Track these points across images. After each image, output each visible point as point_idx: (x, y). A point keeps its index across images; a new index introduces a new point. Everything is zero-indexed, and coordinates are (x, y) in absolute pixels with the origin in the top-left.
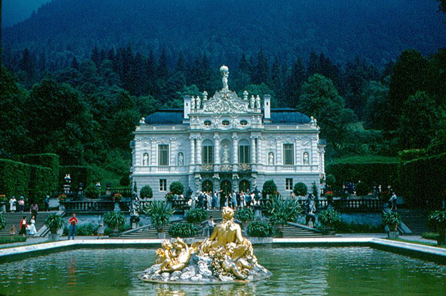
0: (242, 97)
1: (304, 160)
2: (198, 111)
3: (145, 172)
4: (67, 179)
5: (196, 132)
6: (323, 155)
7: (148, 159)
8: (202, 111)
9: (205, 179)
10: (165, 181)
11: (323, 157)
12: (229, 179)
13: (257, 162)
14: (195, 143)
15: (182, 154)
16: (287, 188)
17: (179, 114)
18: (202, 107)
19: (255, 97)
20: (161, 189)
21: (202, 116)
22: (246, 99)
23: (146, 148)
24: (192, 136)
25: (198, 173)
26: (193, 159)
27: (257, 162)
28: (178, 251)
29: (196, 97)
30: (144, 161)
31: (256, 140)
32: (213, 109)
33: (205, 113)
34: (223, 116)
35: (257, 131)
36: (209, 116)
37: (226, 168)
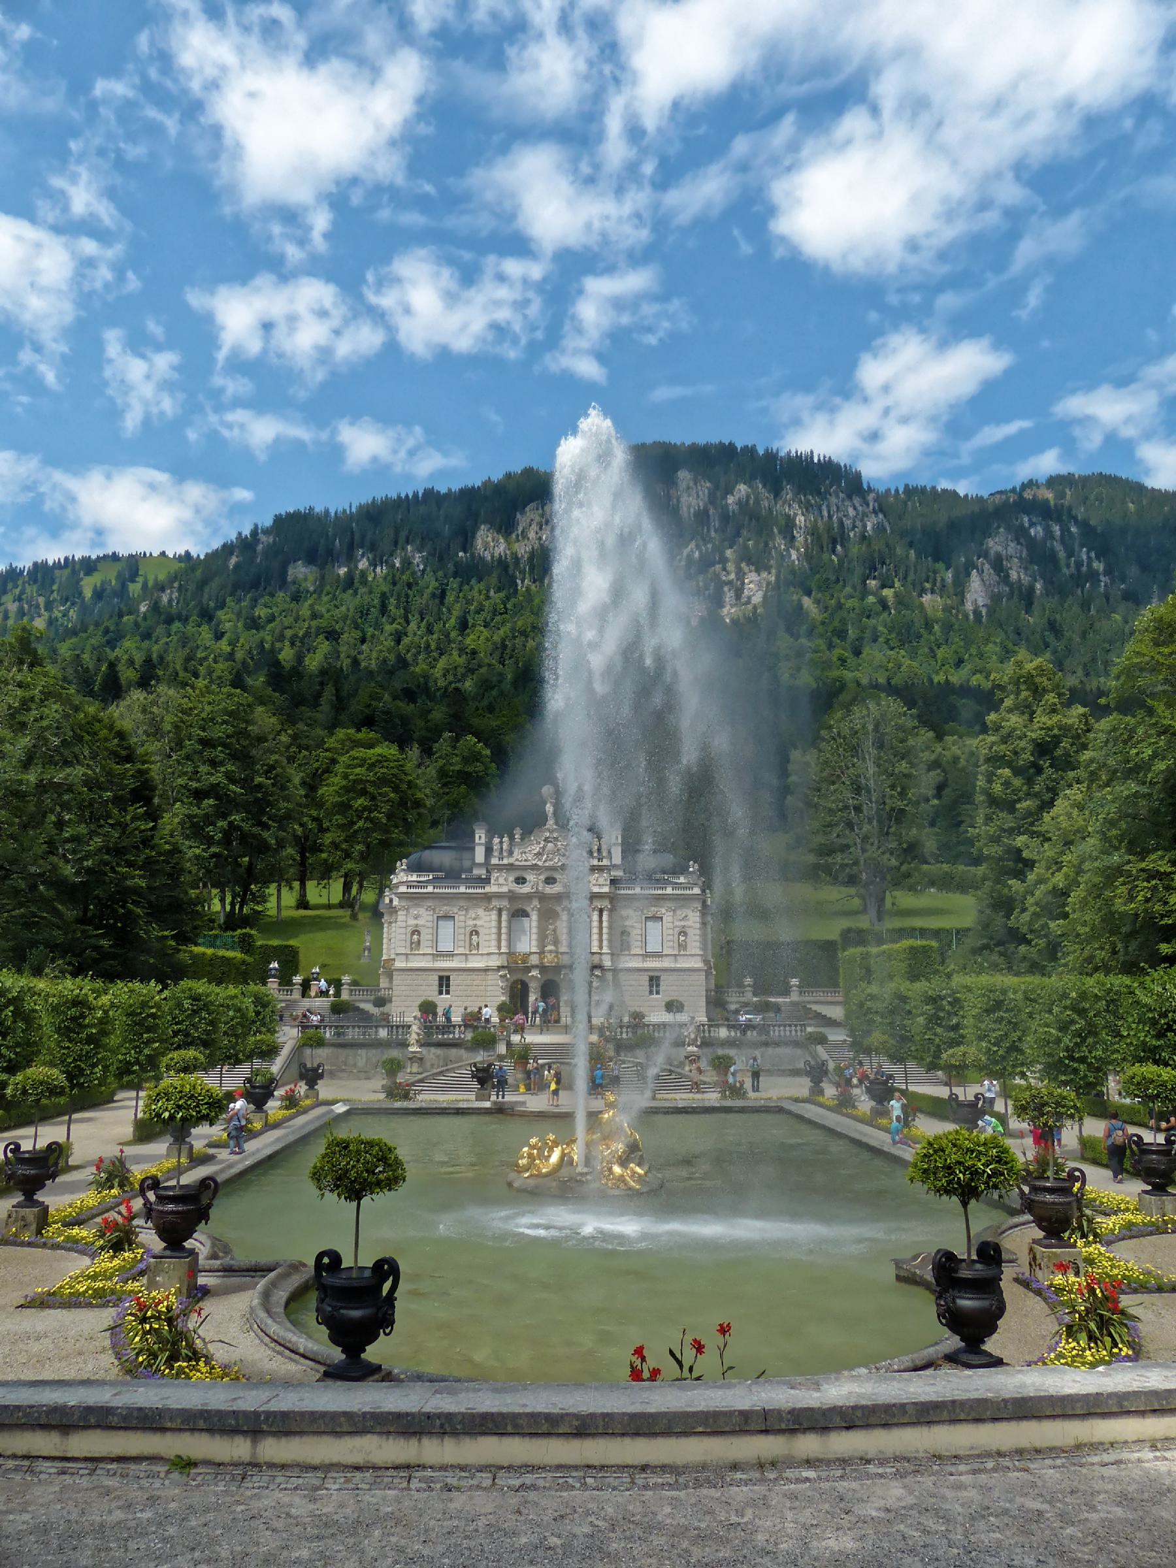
2: (505, 861)
4: (275, 969)
5: (499, 896)
7: (419, 941)
8: (511, 860)
9: (515, 978)
10: (448, 978)
12: (556, 978)
13: (601, 947)
14: (500, 916)
15: (477, 933)
16: (651, 992)
17: (466, 855)
18: (511, 853)
20: (441, 993)
21: (511, 867)
24: (495, 903)
25: (503, 967)
26: (494, 943)
27: (601, 947)
28: (551, 1150)
30: (412, 943)
31: (601, 911)
33: (517, 863)
36: (525, 868)
37: (549, 959)
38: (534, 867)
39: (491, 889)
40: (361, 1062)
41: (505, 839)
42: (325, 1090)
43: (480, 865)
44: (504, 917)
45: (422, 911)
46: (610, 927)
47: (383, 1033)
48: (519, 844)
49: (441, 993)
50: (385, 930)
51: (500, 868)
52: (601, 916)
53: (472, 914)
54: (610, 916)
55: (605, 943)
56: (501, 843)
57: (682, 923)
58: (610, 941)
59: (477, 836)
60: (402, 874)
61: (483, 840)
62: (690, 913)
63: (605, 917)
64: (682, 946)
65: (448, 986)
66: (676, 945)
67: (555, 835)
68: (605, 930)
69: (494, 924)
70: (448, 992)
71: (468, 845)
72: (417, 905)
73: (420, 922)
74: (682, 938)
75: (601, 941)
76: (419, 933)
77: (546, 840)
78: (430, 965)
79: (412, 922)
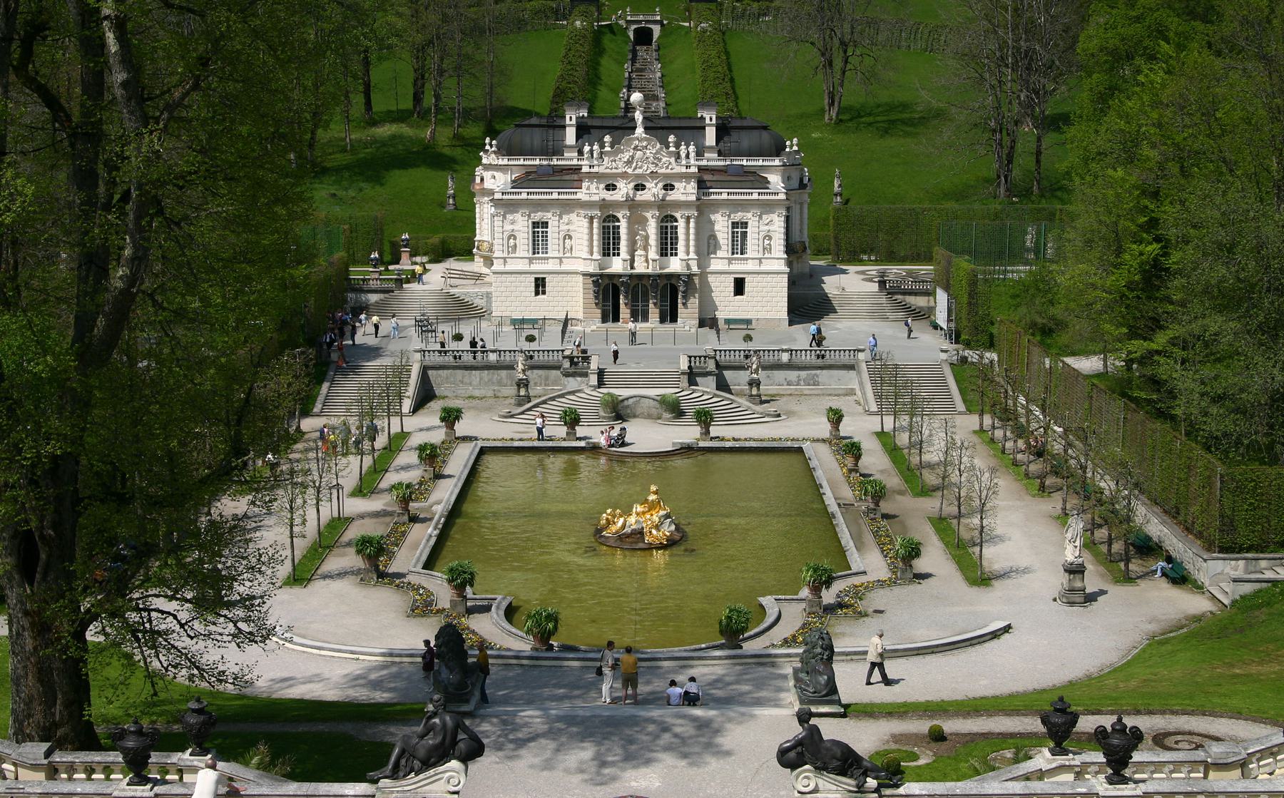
0: (668, 147)
1: (764, 249)
2: (596, 169)
3: (513, 266)
6: (806, 206)
8: (601, 170)
11: (806, 211)
14: (591, 223)
15: (570, 237)
19: (688, 146)
20: (537, 293)
21: (598, 177)
22: (672, 149)
23: (511, 227)
26: (586, 249)
29: (591, 145)
31: (688, 219)
32: (620, 164)
34: (638, 176)
35: (686, 205)
38: (624, 175)
39: (582, 195)
40: (476, 381)
41: (596, 147)
42: (461, 428)
43: (571, 147)
44: (595, 225)
45: (518, 216)
46: (697, 234)
47: (493, 357)
48: (607, 153)
49: (537, 293)
50: (477, 210)
51: (592, 176)
52: (688, 222)
53: (565, 218)
54: (697, 223)
55: (692, 249)
56: (591, 152)
57: (767, 228)
58: (697, 246)
59: (568, 117)
60: (493, 156)
61: (574, 122)
62: (774, 217)
63: (692, 224)
64: (767, 249)
65: (544, 286)
66: (761, 249)
67: (645, 144)
68: (692, 237)
69: (586, 231)
70: (544, 293)
71: (559, 122)
72: (512, 212)
73: (515, 227)
74: (767, 242)
75: (687, 246)
76: (515, 238)
77: (636, 148)
78: (526, 268)
79: (508, 227)
